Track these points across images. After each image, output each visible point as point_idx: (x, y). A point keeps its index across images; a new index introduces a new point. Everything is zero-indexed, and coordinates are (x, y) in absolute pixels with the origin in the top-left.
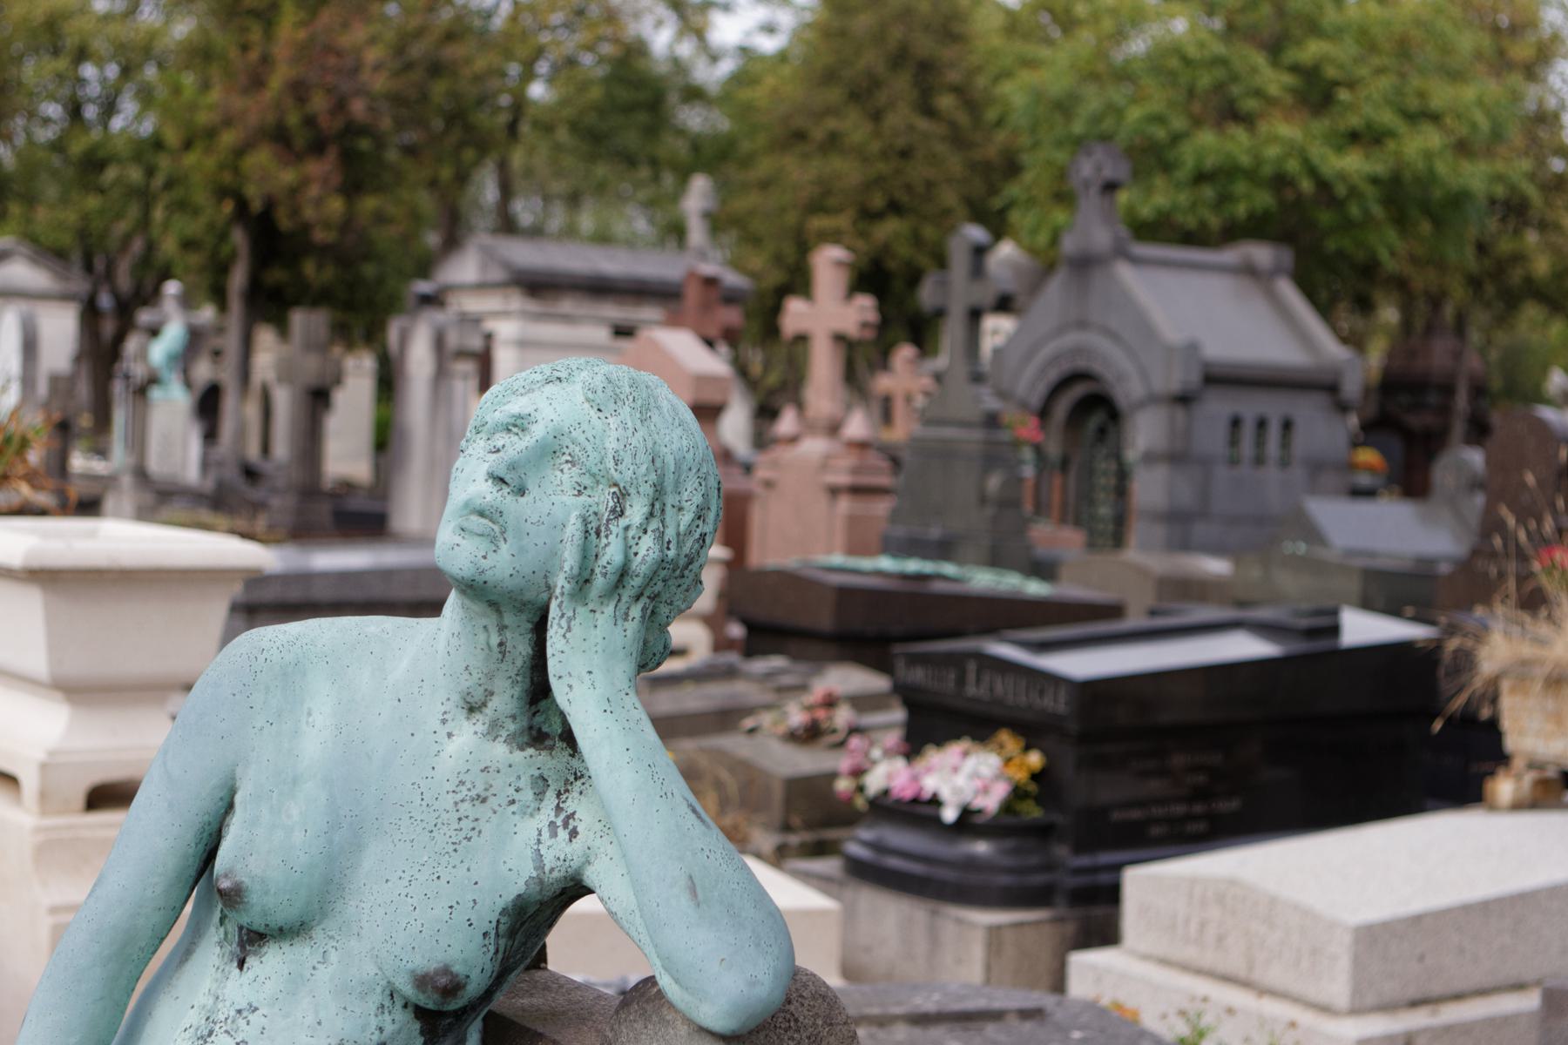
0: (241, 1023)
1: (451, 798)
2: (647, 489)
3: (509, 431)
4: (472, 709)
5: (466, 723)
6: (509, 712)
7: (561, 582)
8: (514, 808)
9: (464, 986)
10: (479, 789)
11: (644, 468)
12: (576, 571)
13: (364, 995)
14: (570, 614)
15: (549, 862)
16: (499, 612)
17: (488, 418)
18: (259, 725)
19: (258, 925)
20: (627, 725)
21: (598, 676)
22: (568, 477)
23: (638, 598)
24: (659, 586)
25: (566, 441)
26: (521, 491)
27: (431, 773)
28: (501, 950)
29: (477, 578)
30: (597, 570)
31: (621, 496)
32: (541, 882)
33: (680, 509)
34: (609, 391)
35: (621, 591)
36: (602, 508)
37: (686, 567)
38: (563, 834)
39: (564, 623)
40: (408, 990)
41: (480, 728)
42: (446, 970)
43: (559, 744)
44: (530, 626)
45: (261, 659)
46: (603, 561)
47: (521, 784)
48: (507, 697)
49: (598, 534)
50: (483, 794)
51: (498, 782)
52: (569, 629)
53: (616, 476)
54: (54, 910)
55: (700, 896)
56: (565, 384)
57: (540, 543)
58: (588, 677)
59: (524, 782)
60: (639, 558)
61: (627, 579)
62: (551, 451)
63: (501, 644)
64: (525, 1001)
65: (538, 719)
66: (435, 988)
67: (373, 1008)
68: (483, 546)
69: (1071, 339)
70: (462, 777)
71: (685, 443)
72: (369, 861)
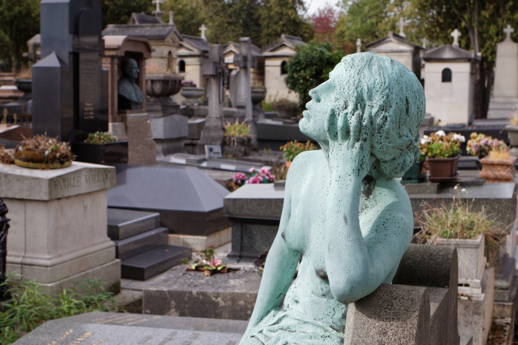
11: (351, 92)
14: (333, 145)
20: (341, 186)
33: (373, 107)
34: (351, 64)
52: (333, 151)
57: (320, 119)
58: (336, 168)
71: (377, 81)
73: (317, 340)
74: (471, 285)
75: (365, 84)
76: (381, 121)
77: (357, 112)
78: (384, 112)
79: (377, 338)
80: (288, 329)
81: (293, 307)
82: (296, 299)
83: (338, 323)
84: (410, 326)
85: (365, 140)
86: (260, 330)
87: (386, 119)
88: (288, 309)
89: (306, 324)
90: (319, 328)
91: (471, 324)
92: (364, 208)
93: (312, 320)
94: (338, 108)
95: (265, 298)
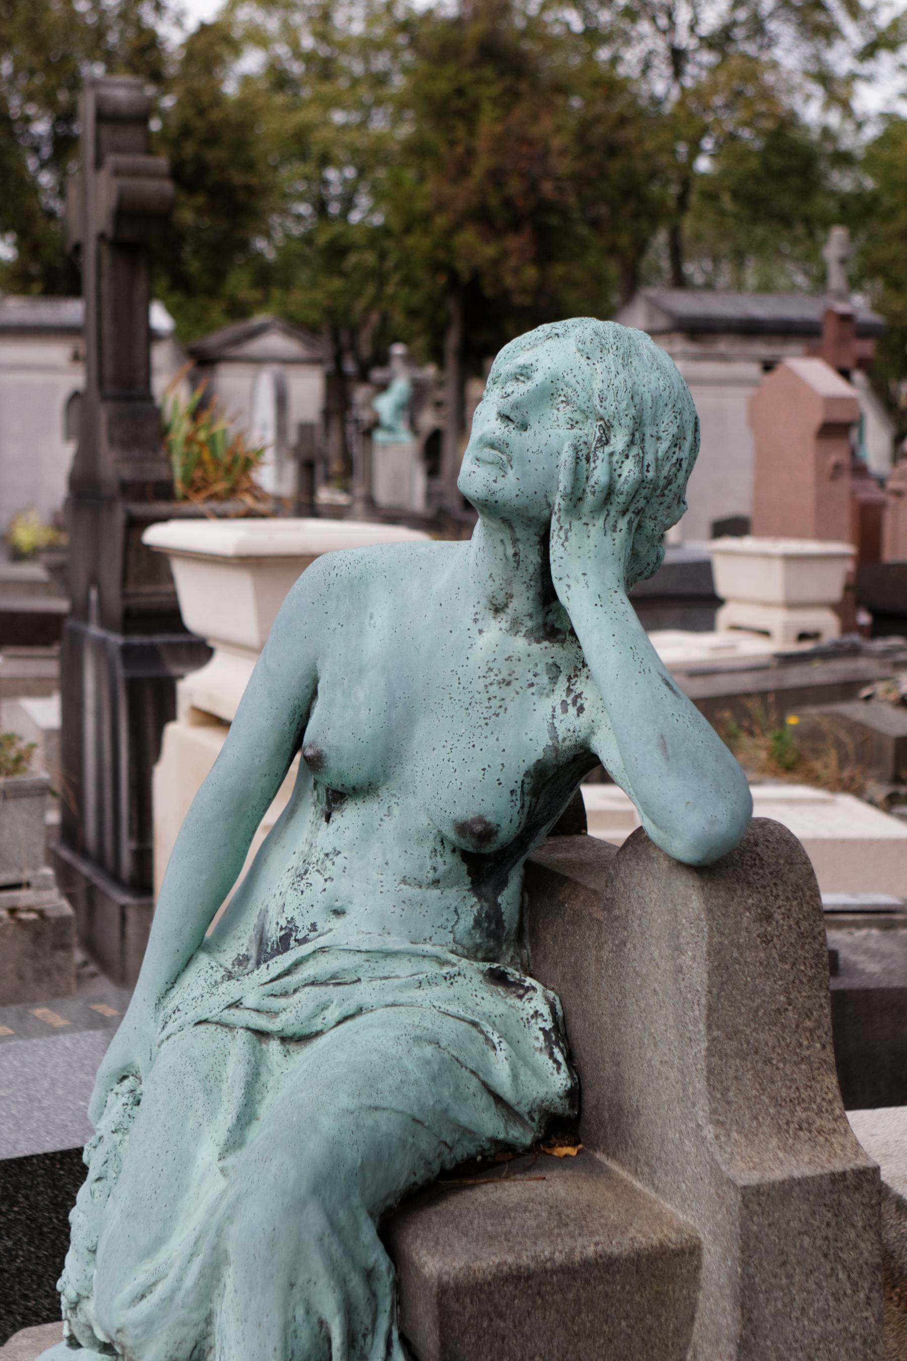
0: (328, 863)
2: (627, 421)
3: (518, 379)
4: (498, 609)
5: (493, 622)
6: (526, 612)
7: (558, 501)
8: (533, 690)
9: (496, 833)
10: (504, 674)
11: (625, 403)
12: (569, 490)
13: (420, 841)
14: (567, 526)
15: (561, 733)
16: (511, 527)
17: (501, 371)
18: (332, 627)
19: (336, 784)
21: (591, 577)
22: (563, 413)
23: (624, 513)
24: (642, 503)
25: (561, 385)
26: (524, 427)
27: (465, 662)
28: (527, 804)
29: (490, 498)
30: (588, 490)
31: (607, 428)
32: (556, 749)
33: (659, 438)
35: (609, 507)
36: (591, 438)
37: (666, 487)
38: (572, 710)
39: (562, 534)
40: (452, 835)
41: (505, 625)
42: (481, 820)
44: (537, 539)
45: (333, 574)
46: (592, 482)
47: (539, 670)
48: (523, 599)
49: (588, 460)
50: (508, 679)
51: (519, 669)
52: (567, 539)
53: (602, 411)
55: (670, 752)
56: (561, 339)
57: (540, 468)
58: (582, 578)
59: (541, 668)
60: (623, 478)
61: (614, 497)
62: (549, 393)
63: (515, 555)
64: (561, 856)
65: (551, 617)
66: (473, 834)
67: (427, 851)
68: (494, 472)
70: (491, 665)
71: (661, 383)
73: (435, 989)
74: (34, 883)
75: (644, 389)
76: (674, 469)
77: (635, 450)
78: (677, 450)
79: (757, 929)
80: (335, 980)
81: (330, 926)
82: (338, 905)
83: (465, 942)
84: (808, 893)
85: (637, 513)
86: (231, 1001)
87: (680, 465)
88: (312, 935)
89: (389, 960)
90: (426, 960)
91: (49, 973)
92: (580, 666)
93: (407, 946)
94: (585, 443)
95: (189, 926)
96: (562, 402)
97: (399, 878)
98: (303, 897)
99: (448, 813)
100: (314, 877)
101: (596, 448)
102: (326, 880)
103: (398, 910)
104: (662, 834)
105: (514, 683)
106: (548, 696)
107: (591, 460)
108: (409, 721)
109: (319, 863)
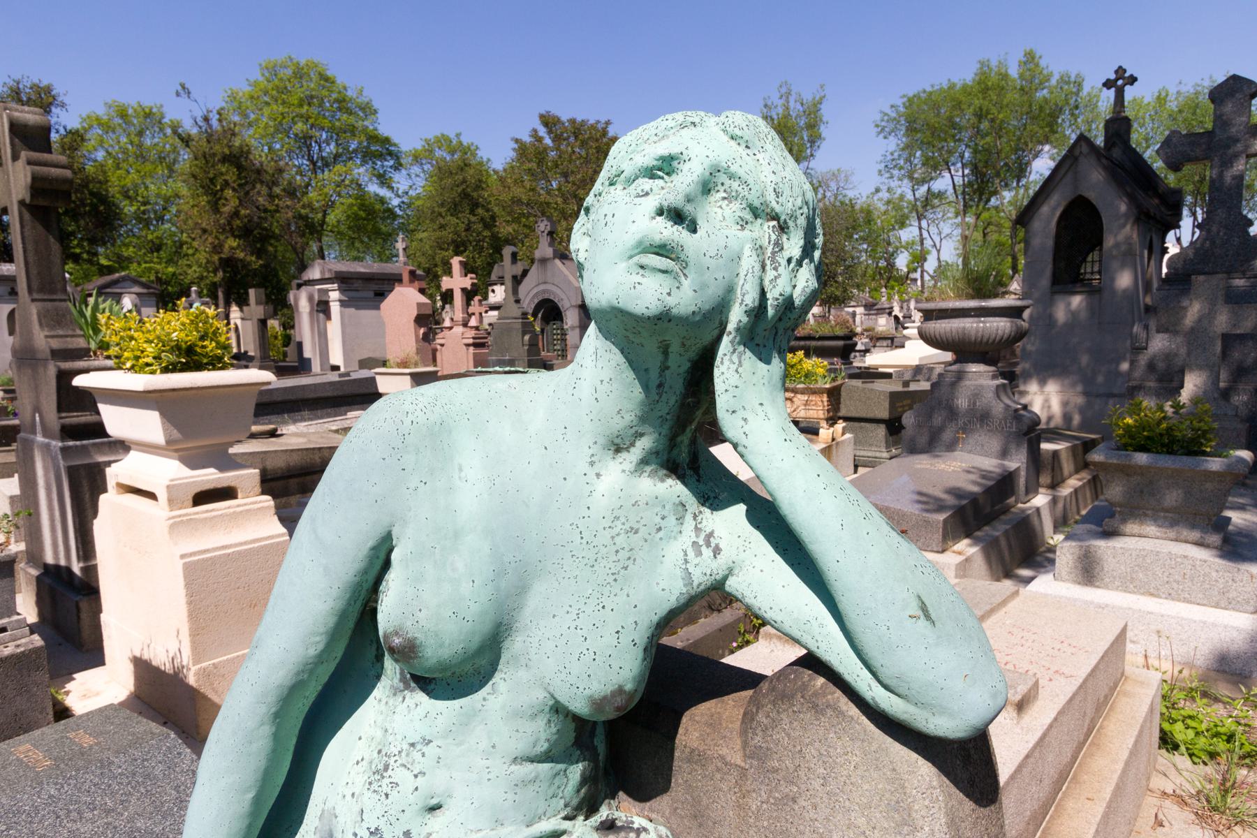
0: (416, 755)
1: (608, 533)
2: (802, 221)
4: (618, 450)
8: (661, 534)
13: (534, 716)
17: (623, 167)
18: (412, 486)
27: (587, 513)
38: (707, 553)
43: (689, 472)
45: (407, 422)
52: (740, 364)
53: (778, 209)
54: (182, 557)
55: (933, 616)
56: (699, 128)
58: (760, 409)
69: (542, 287)
70: (616, 513)
72: (534, 602)
82: (434, 802)
96: (724, 198)
97: (508, 760)
98: (389, 801)
99: (581, 689)
100: (399, 774)
101: (773, 253)
102: (416, 776)
103: (510, 796)
104: (911, 709)
105: (642, 529)
106: (675, 538)
107: (768, 268)
108: (522, 590)
109: (403, 754)
